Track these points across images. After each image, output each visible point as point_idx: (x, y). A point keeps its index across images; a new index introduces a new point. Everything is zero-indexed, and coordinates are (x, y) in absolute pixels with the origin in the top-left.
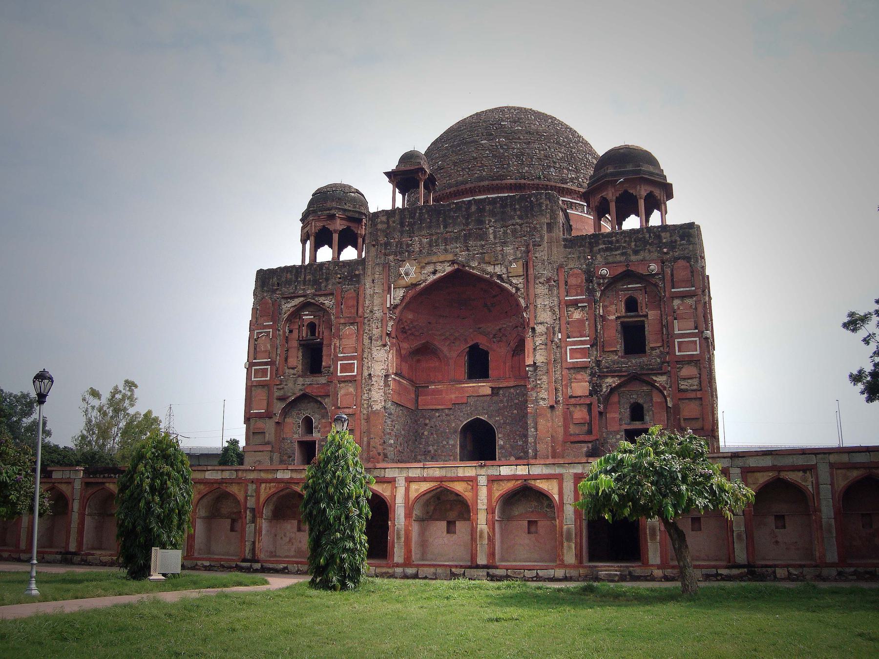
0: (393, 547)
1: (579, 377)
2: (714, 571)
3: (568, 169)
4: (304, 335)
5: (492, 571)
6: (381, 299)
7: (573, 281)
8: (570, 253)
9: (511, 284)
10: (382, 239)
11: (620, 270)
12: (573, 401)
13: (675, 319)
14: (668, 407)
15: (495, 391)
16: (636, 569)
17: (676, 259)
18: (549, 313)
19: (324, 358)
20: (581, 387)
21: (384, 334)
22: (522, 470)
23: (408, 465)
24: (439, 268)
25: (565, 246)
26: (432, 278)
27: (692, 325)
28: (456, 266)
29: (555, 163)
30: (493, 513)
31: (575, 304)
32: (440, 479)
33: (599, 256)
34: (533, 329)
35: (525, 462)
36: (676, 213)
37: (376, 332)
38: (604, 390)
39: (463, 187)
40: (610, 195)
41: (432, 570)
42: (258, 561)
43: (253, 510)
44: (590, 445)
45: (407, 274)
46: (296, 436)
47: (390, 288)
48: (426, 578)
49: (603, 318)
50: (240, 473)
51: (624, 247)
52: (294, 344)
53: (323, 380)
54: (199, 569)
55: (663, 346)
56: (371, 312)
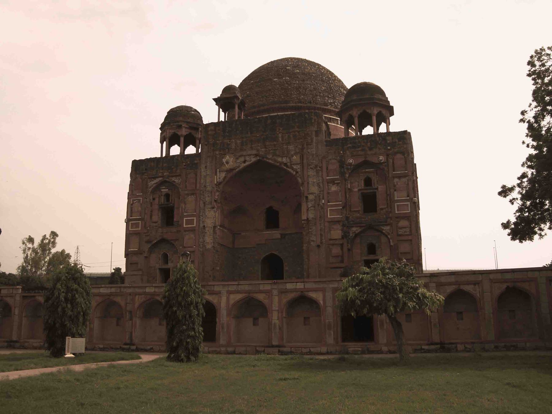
1: (335, 227)
2: (419, 347)
3: (328, 97)
4: (162, 201)
5: (281, 349)
6: (211, 178)
7: (331, 167)
9: (293, 169)
11: (361, 160)
12: (331, 242)
13: (395, 191)
14: (391, 246)
15: (283, 236)
16: (371, 346)
18: (316, 187)
20: (337, 233)
21: (213, 201)
22: (300, 286)
24: (247, 158)
26: (243, 165)
27: (405, 194)
29: (320, 93)
30: (282, 312)
31: (333, 182)
32: (249, 292)
33: (348, 152)
34: (307, 197)
35: (302, 280)
36: (396, 125)
37: (208, 199)
38: (351, 235)
39: (262, 108)
42: (134, 345)
43: (130, 312)
44: (342, 269)
45: (227, 163)
48: (240, 354)
50: (122, 290)
52: (156, 207)
53: (174, 230)
55: (387, 207)
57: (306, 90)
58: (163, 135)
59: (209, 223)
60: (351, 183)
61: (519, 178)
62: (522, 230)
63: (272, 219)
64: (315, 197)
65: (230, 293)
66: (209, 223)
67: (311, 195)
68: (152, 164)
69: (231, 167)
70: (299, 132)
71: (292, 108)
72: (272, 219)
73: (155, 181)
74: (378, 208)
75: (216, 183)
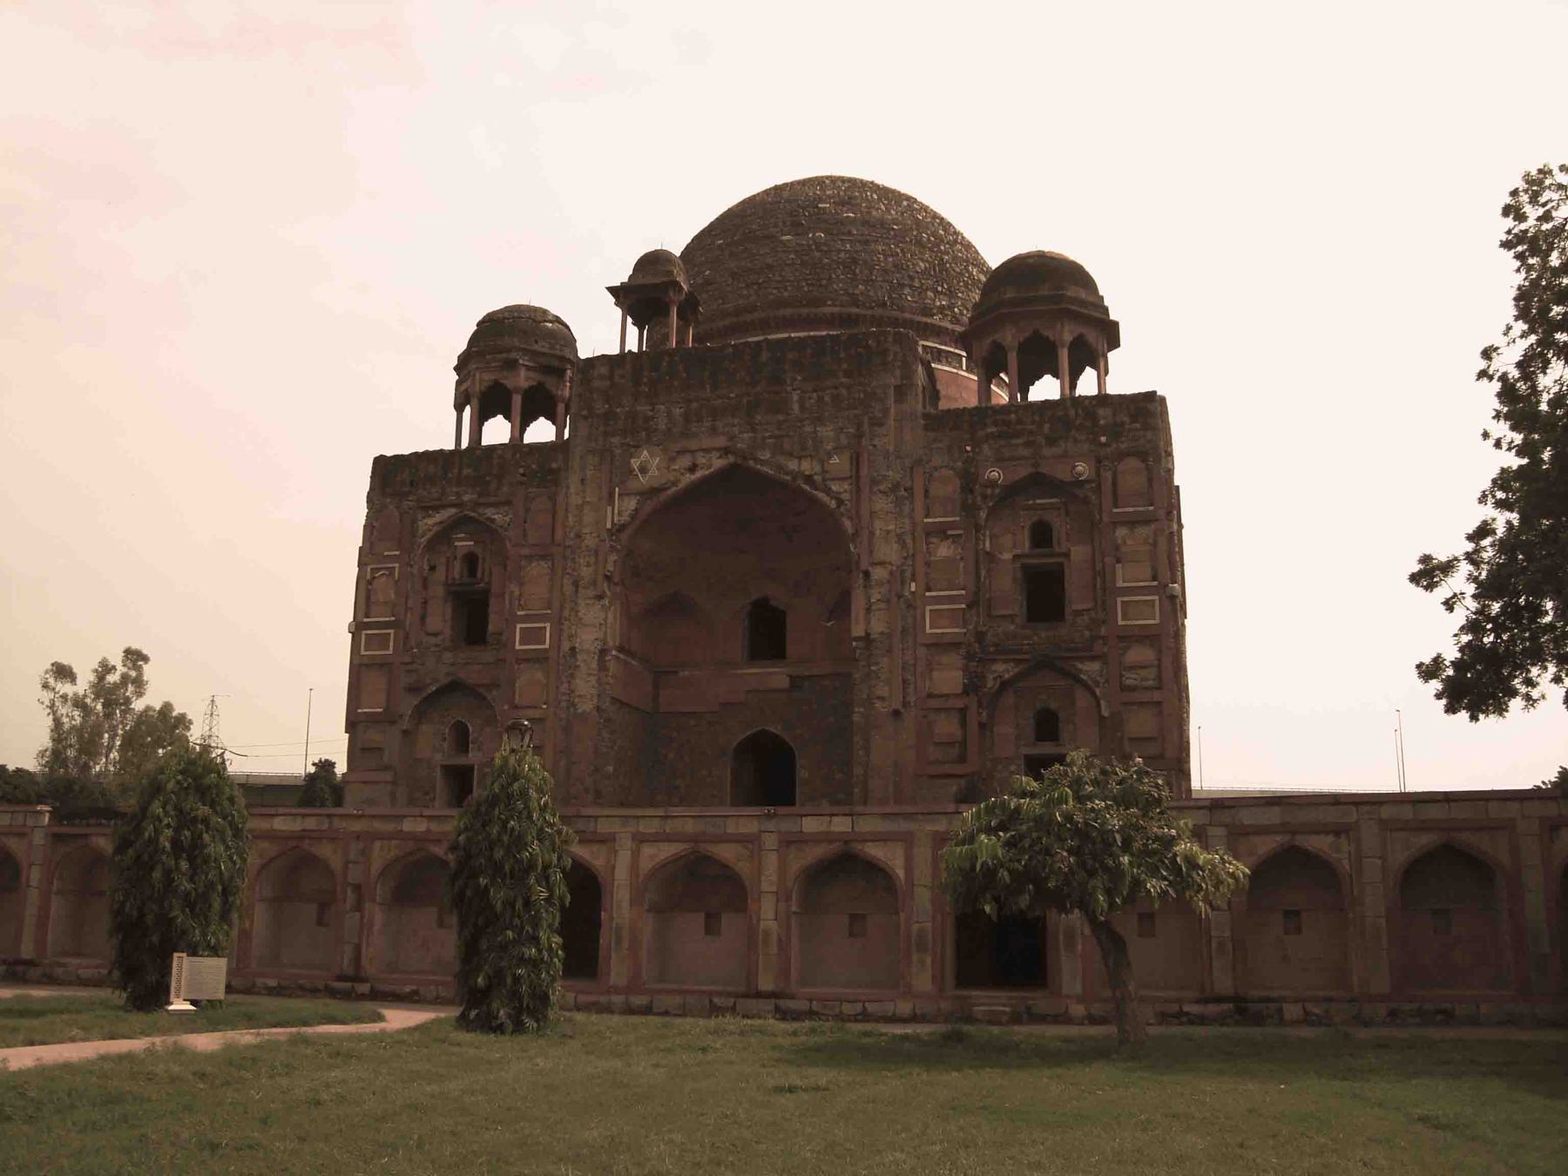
1: (945, 659)
2: (1175, 1008)
3: (936, 292)
5: (783, 1003)
6: (596, 513)
7: (938, 490)
8: (935, 440)
9: (828, 491)
10: (600, 407)
11: (1023, 471)
12: (934, 703)
13: (1118, 561)
14: (1102, 718)
16: (1039, 1001)
17: (1121, 456)
18: (895, 546)
20: (949, 677)
21: (600, 578)
22: (841, 825)
23: (639, 812)
24: (701, 460)
25: (926, 428)
26: (689, 478)
27: (1148, 573)
28: (731, 459)
29: (911, 278)
30: (788, 899)
31: (941, 532)
32: (695, 839)
33: (985, 447)
34: (867, 574)
35: (846, 809)
36: (1124, 374)
38: (990, 684)
39: (748, 317)
40: (1009, 338)
41: (678, 1000)
42: (362, 980)
43: (358, 888)
44: (963, 782)
45: (643, 470)
46: (438, 757)
47: (611, 495)
48: (666, 1013)
50: (337, 823)
51: (1031, 432)
52: (439, 591)
53: (487, 656)
54: (259, 993)
57: (871, 270)
58: (463, 387)
59: (587, 639)
61: (1470, 538)
62: (1476, 684)
63: (767, 634)
64: (891, 573)
65: (641, 839)
66: (587, 639)
68: (432, 469)
70: (848, 388)
71: (830, 321)
72: (767, 634)
73: (438, 518)
74: (1068, 610)
75: (609, 526)
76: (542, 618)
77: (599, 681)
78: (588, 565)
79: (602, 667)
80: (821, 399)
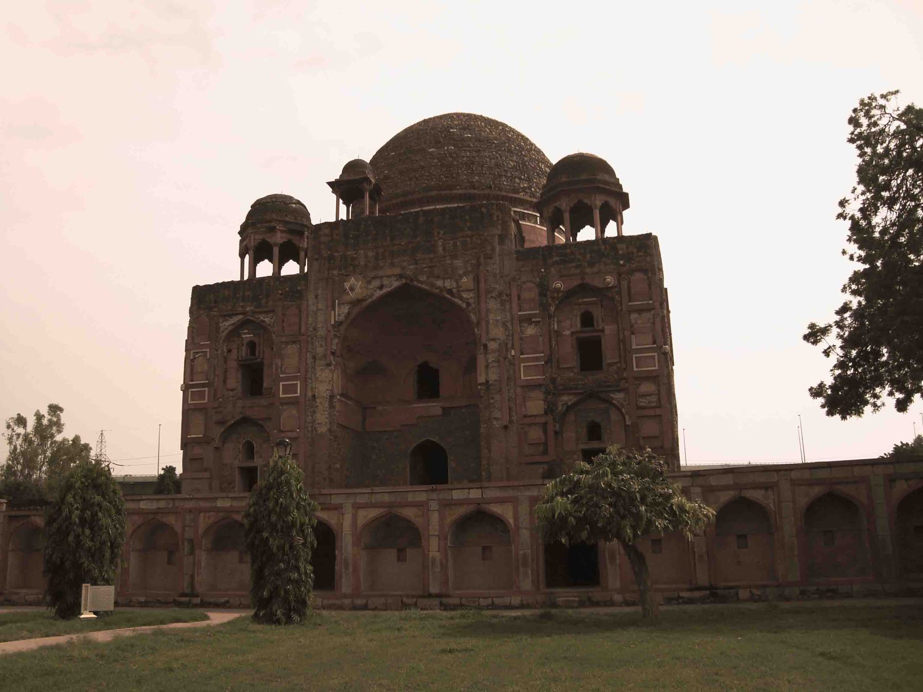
0: (341, 577)
2: (675, 595)
3: (520, 179)
6: (325, 315)
7: (526, 295)
9: (461, 298)
11: (576, 282)
12: (527, 421)
14: (626, 426)
16: (596, 593)
17: (632, 272)
19: (265, 378)
20: (536, 405)
22: (475, 494)
24: (386, 282)
25: (518, 259)
26: (379, 293)
27: (649, 338)
28: (404, 281)
30: (446, 539)
31: (529, 320)
32: (390, 505)
33: (553, 270)
34: (485, 346)
35: (478, 485)
36: (633, 224)
37: (320, 351)
41: (382, 600)
42: (197, 596)
43: (191, 541)
44: (545, 466)
45: (352, 289)
48: (375, 609)
49: (558, 334)
50: (177, 503)
51: (579, 260)
52: (233, 364)
53: (263, 402)
54: (134, 606)
55: (620, 362)
56: (315, 329)
57: (482, 166)
58: (245, 243)
59: (322, 389)
60: (559, 322)
61: (837, 313)
62: (844, 398)
63: (428, 383)
65: (357, 507)
66: (322, 389)
67: (493, 343)
68: (226, 292)
69: (360, 297)
71: (461, 198)
72: (428, 383)
75: (333, 322)
76: (296, 378)
77: (330, 414)
78: (321, 346)
79: (332, 406)
80: (455, 245)
